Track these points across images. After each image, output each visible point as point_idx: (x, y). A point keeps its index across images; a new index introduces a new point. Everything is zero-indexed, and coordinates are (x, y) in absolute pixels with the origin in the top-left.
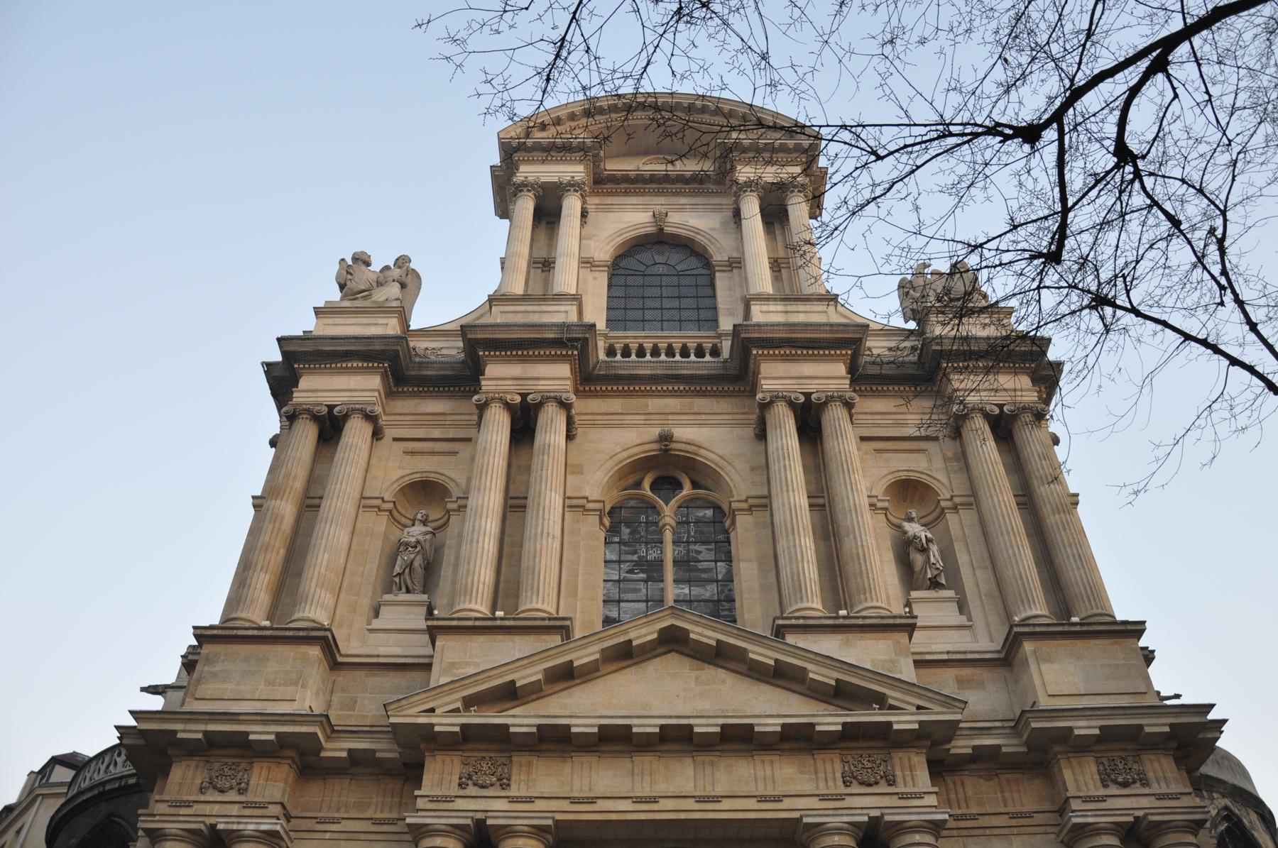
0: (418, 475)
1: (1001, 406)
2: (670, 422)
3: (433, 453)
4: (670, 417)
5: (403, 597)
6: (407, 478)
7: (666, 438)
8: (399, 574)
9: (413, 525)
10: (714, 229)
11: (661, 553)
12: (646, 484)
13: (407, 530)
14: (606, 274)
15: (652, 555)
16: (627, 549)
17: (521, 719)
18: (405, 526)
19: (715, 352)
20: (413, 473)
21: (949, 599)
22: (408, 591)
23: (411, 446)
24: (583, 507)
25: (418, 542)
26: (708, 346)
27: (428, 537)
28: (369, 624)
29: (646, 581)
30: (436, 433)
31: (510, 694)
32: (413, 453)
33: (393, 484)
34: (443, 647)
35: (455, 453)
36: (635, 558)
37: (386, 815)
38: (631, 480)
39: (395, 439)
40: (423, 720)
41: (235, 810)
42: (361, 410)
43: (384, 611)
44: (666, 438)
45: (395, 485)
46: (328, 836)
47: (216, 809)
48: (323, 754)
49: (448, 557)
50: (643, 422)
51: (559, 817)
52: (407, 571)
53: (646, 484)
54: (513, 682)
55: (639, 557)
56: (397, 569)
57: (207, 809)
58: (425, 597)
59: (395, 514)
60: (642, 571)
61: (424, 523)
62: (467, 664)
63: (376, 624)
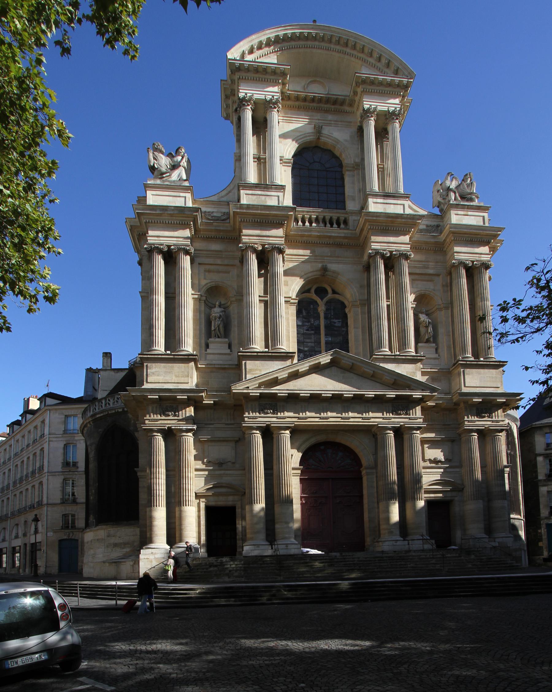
0: (214, 283)
1: (473, 262)
2: (325, 261)
3: (218, 272)
4: (326, 258)
5: (217, 340)
6: (209, 285)
7: (325, 269)
8: (214, 330)
9: (215, 307)
11: (320, 322)
12: (313, 291)
13: (213, 309)
14: (290, 168)
15: (316, 323)
16: (306, 320)
17: (281, 390)
18: (212, 308)
19: (346, 222)
20: (211, 282)
22: (219, 337)
23: (208, 267)
24: (289, 301)
25: (220, 316)
26: (342, 219)
27: (223, 313)
28: (206, 351)
29: (314, 334)
30: (219, 262)
31: (276, 382)
32: (209, 271)
33: (203, 287)
34: (245, 363)
35: (229, 272)
37: (229, 422)
38: (307, 288)
39: (199, 264)
42: (184, 249)
43: (211, 346)
44: (325, 269)
45: (205, 288)
46: (209, 429)
48: (204, 402)
49: (235, 322)
50: (313, 260)
51: (296, 423)
52: (217, 328)
53: (313, 291)
54: (277, 377)
55: (311, 324)
56: (213, 328)
58: (227, 340)
59: (207, 302)
60: (312, 330)
61: (220, 306)
62: (256, 370)
63: (209, 351)
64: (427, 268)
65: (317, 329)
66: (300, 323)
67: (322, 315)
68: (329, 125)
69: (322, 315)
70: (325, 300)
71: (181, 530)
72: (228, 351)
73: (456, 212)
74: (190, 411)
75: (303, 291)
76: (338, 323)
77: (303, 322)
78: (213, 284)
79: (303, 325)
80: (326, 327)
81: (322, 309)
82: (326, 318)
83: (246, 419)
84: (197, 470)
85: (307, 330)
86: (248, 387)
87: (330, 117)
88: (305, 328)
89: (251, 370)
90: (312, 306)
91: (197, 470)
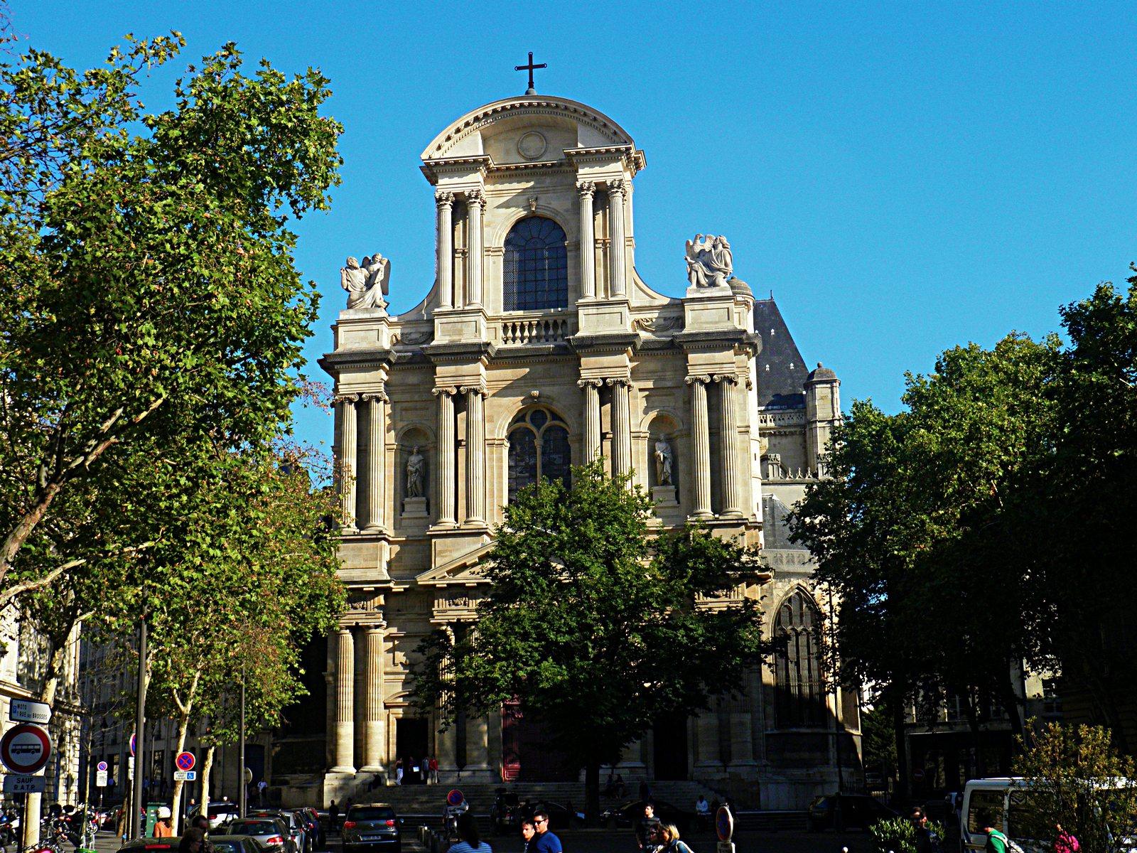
10: (567, 211)
12: (528, 418)
15: (532, 462)
21: (670, 491)
22: (416, 496)
23: (405, 405)
30: (416, 398)
32: (406, 410)
36: (523, 464)
40: (432, 583)
41: (364, 616)
43: (407, 508)
47: (357, 616)
49: (432, 477)
53: (528, 418)
56: (409, 485)
57: (354, 616)
63: (404, 515)
64: (664, 379)
65: (533, 468)
66: (513, 464)
67: (539, 451)
68: (547, 192)
69: (539, 451)
70: (542, 429)
71: (366, 750)
72: (425, 514)
73: (691, 307)
74: (381, 600)
75: (519, 418)
76: (558, 459)
77: (516, 462)
78: (410, 427)
79: (516, 466)
80: (544, 466)
81: (538, 443)
82: (543, 453)
83: (435, 613)
84: (386, 673)
85: (521, 472)
86: (434, 578)
87: (548, 180)
88: (518, 469)
89: (440, 552)
90: (527, 439)
91: (386, 673)
